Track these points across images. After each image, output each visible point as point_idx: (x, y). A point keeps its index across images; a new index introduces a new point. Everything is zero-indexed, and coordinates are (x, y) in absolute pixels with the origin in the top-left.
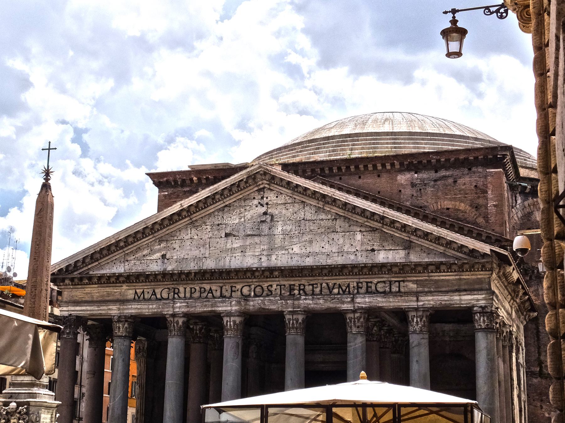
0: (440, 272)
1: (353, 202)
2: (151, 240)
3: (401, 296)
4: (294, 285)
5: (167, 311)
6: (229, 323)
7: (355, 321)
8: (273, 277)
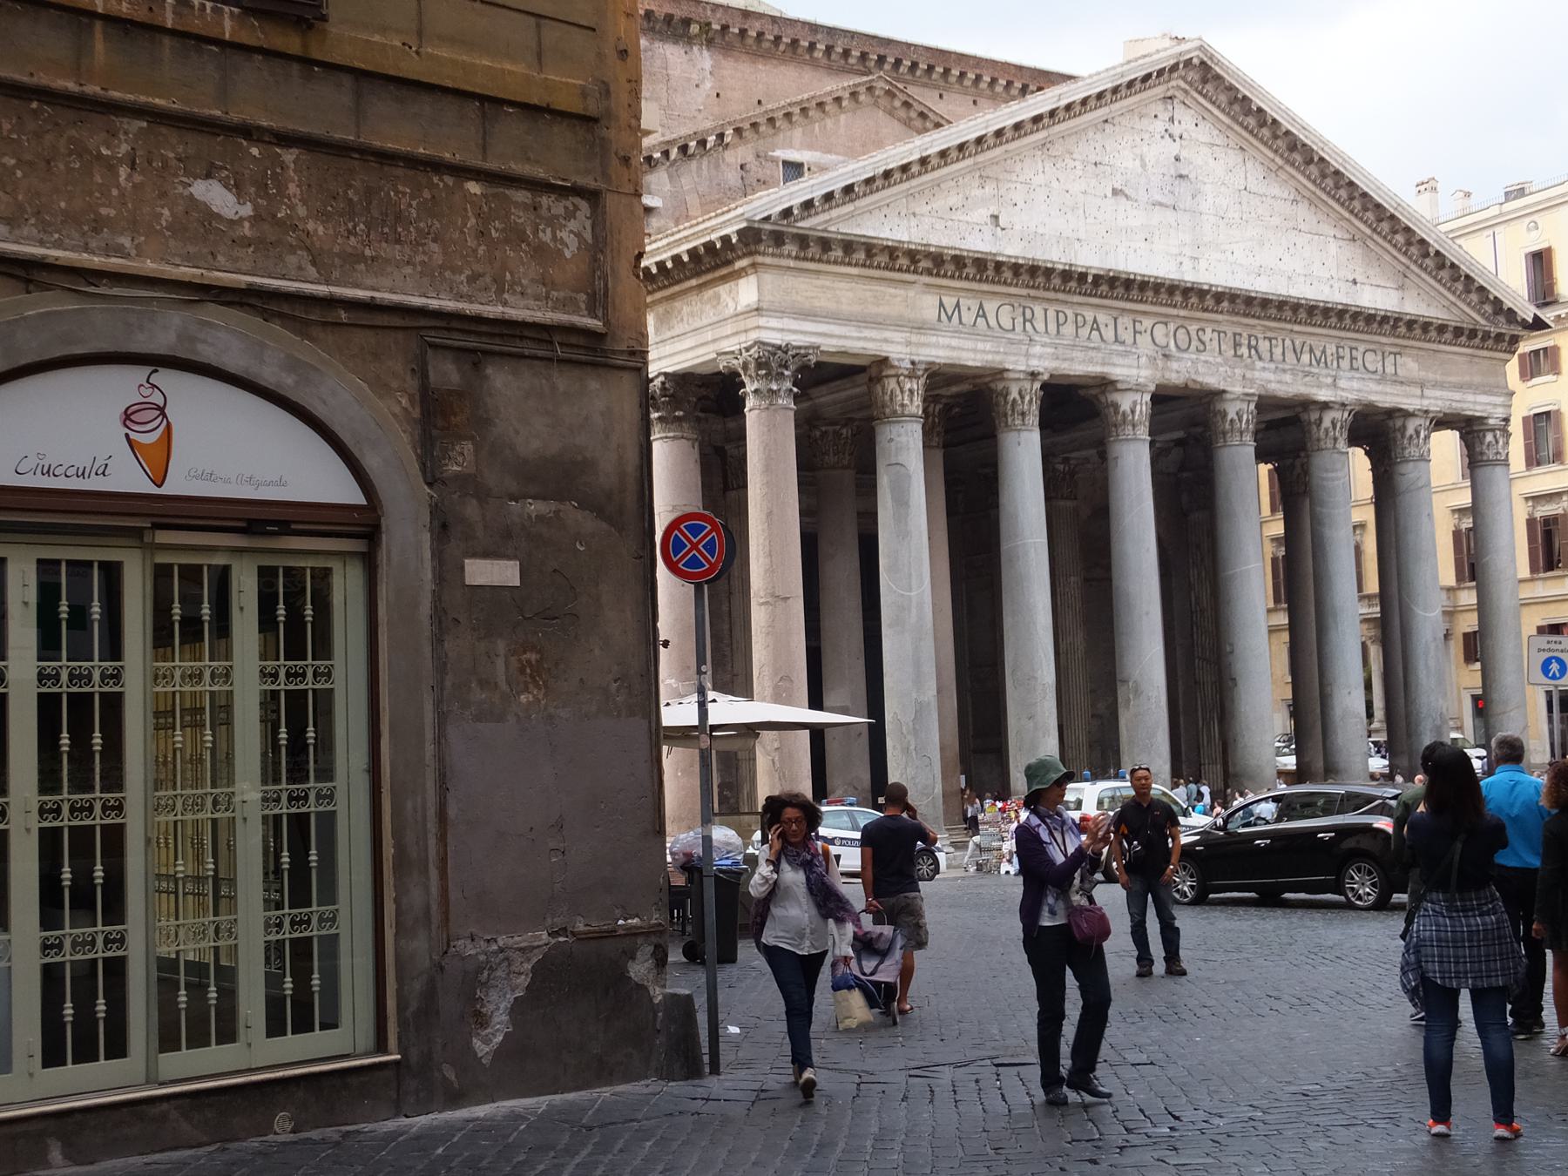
0: (1455, 345)
1: (1350, 172)
2: (963, 172)
3: (1402, 383)
4: (1240, 335)
5: (1017, 363)
6: (1138, 408)
7: (1341, 428)
8: (1216, 312)
